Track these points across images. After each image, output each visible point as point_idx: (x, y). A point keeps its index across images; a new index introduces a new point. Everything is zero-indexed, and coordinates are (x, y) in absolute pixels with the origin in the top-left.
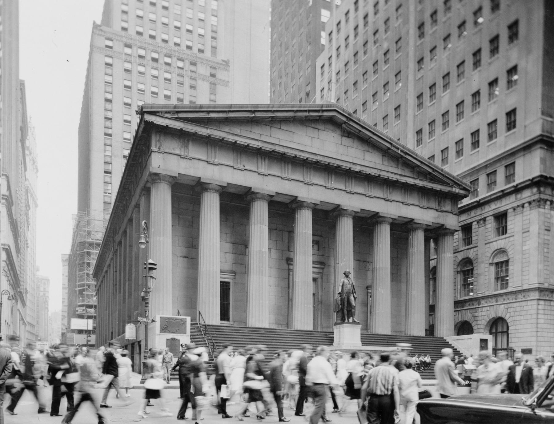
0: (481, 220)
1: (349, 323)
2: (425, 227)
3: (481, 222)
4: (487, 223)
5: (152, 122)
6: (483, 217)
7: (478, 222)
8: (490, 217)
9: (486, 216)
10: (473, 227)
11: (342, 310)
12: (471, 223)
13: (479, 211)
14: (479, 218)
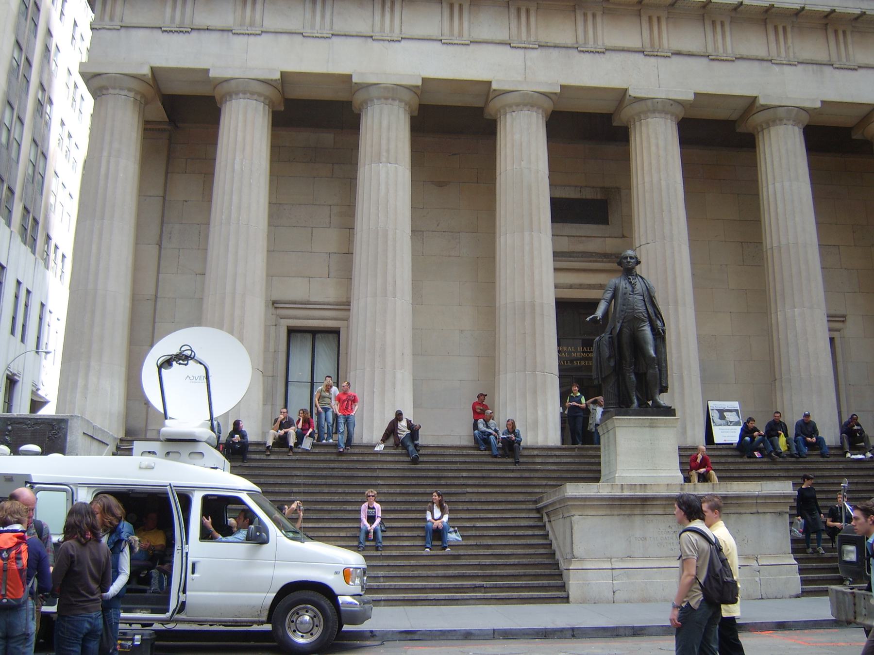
11: (619, 371)
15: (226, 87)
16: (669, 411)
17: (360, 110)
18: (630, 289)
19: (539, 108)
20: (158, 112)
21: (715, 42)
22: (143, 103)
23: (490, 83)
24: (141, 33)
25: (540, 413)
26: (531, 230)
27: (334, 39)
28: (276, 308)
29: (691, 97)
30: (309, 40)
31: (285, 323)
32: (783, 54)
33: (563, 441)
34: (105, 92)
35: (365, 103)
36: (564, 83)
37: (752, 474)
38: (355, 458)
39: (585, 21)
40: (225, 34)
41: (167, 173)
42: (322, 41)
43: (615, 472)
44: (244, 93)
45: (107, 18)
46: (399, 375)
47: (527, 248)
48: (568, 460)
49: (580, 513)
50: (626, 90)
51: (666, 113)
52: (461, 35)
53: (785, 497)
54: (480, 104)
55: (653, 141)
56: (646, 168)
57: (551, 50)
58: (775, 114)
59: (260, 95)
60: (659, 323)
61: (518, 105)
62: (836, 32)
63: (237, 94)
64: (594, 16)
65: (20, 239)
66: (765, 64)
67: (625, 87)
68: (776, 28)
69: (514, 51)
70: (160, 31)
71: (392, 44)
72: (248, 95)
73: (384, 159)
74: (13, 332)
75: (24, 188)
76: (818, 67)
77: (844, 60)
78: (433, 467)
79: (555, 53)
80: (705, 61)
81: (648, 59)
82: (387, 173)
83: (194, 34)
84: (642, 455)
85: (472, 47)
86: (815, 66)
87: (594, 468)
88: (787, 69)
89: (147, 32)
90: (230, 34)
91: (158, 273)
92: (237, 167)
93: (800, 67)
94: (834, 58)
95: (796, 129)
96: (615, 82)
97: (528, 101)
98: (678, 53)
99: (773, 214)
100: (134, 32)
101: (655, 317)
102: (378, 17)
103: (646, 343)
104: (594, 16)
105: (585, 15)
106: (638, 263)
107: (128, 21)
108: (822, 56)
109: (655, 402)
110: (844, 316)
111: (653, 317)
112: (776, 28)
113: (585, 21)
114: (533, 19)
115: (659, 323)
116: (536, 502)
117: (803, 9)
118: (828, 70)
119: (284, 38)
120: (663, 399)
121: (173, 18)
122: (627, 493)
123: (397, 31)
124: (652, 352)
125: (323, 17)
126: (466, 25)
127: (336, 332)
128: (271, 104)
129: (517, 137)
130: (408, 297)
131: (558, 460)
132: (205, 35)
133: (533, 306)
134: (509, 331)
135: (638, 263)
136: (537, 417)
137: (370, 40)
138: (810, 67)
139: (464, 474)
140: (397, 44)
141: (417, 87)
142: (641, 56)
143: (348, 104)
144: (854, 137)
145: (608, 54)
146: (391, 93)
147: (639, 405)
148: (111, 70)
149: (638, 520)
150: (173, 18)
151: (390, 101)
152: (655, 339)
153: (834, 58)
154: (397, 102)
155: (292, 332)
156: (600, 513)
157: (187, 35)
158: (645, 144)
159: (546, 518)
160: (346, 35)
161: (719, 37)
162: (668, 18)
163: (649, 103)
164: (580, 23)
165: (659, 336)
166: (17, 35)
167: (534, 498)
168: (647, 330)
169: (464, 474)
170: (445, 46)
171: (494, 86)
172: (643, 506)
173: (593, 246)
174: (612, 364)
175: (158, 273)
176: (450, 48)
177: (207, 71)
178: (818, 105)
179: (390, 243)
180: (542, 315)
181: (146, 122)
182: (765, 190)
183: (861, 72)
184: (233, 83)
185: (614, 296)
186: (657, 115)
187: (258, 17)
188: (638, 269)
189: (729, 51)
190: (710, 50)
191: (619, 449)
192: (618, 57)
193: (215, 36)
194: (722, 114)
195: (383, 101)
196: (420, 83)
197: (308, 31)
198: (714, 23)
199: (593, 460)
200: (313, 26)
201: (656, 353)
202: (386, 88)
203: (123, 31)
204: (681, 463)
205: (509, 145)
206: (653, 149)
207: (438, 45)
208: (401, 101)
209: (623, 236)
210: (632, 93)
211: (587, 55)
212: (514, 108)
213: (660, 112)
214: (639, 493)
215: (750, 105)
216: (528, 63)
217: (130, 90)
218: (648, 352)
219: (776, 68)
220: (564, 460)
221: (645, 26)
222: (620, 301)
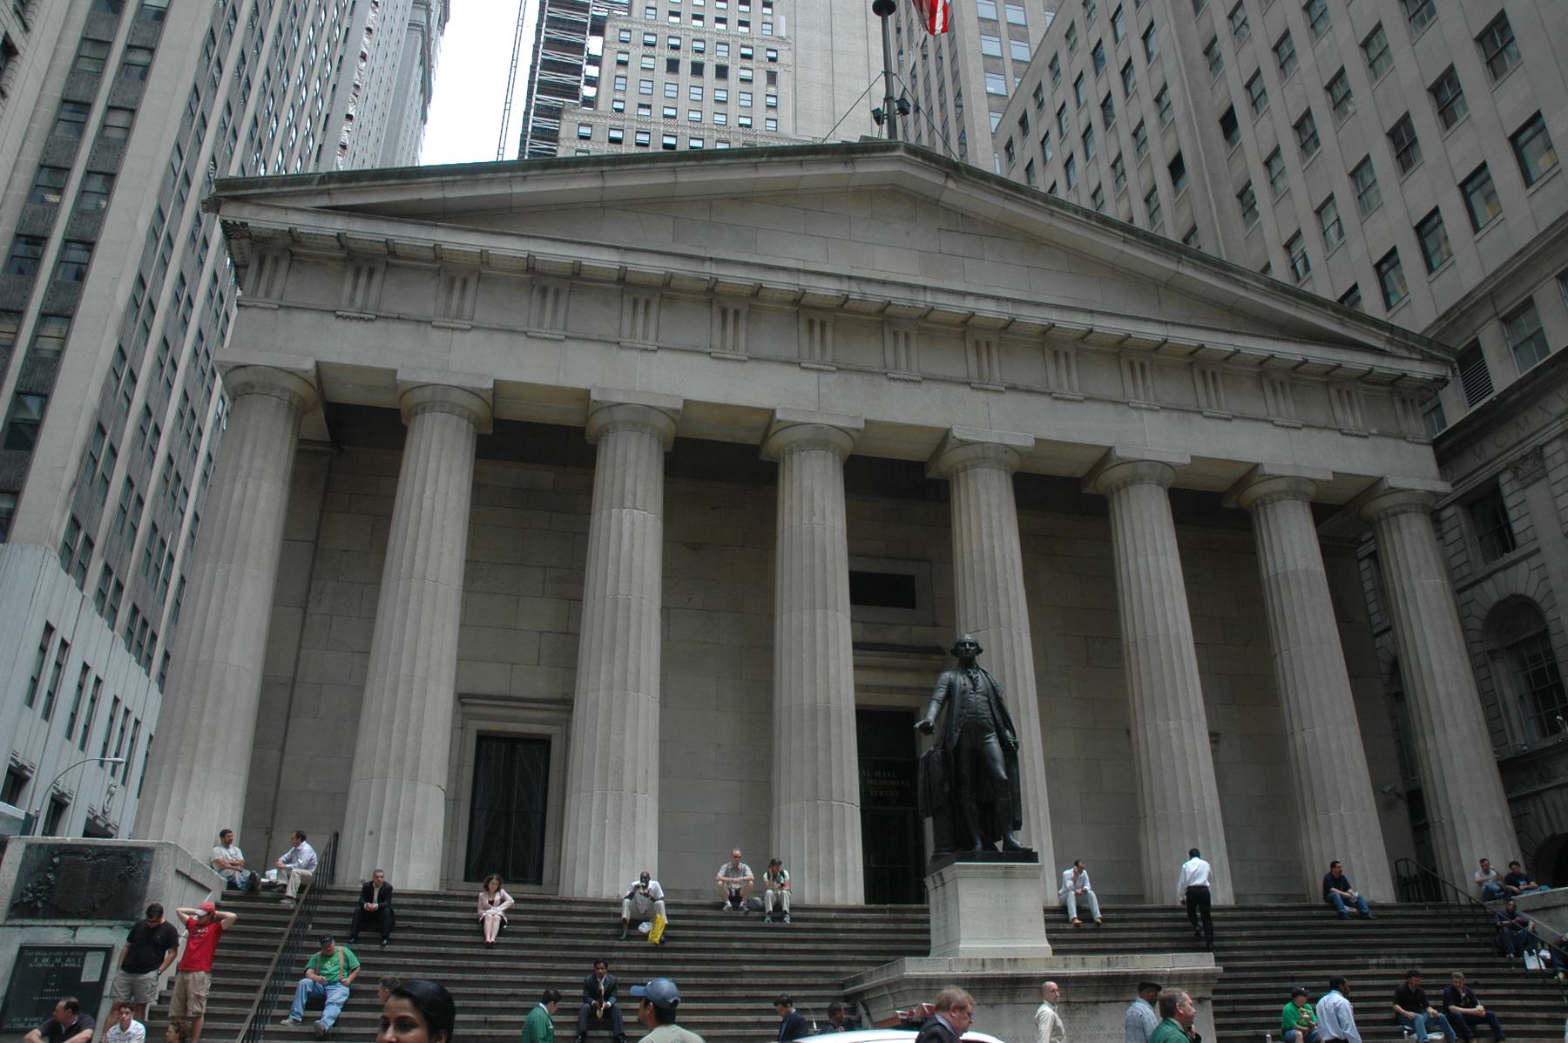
0: (1524, 458)
1: (990, 855)
2: (1311, 489)
3: (1529, 466)
4: (1549, 464)
5: (244, 225)
6: (1528, 449)
7: (1514, 467)
8: (1557, 445)
9: (1540, 442)
10: (1506, 490)
12: (1495, 478)
13: (1508, 436)
14: (1518, 456)
15: (418, 396)
16: (1029, 856)
17: (598, 438)
18: (969, 685)
20: (316, 427)
22: (298, 411)
23: (773, 411)
25: (837, 859)
26: (826, 607)
27: (568, 343)
28: (463, 704)
29: (1030, 443)
31: (475, 726)
32: (1142, 396)
33: (867, 901)
35: (604, 431)
36: (870, 417)
37: (1130, 945)
38: (578, 919)
39: (896, 341)
40: (422, 327)
41: (322, 511)
42: (551, 344)
43: (958, 941)
45: (261, 292)
46: (640, 803)
47: (819, 632)
48: (881, 926)
50: (947, 432)
52: (735, 348)
53: (1206, 976)
54: (753, 440)
56: (974, 532)
60: (1008, 733)
62: (1203, 373)
65: (94, 607)
66: (1120, 408)
67: (947, 426)
68: (1132, 365)
69: (805, 373)
71: (645, 354)
73: (628, 504)
74: (69, 735)
75: (108, 539)
78: (691, 933)
79: (856, 379)
80: (1047, 400)
81: (975, 393)
82: (633, 523)
83: (379, 324)
84: (991, 920)
88: (1146, 415)
91: (300, 648)
92: (427, 503)
93: (1163, 414)
94: (1203, 402)
96: (937, 420)
97: (820, 439)
98: (1013, 388)
99: (1135, 597)
100: (296, 315)
101: (1003, 723)
102: (627, 320)
103: (993, 759)
104: (907, 335)
105: (895, 334)
106: (979, 651)
107: (290, 299)
109: (1009, 845)
111: (1001, 723)
113: (896, 341)
115: (1008, 733)
116: (842, 986)
118: (1197, 419)
119: (501, 338)
120: (1019, 839)
121: (352, 300)
122: (990, 971)
124: (1003, 773)
125: (555, 313)
126: (742, 336)
127: (544, 743)
128: (476, 422)
129: (807, 483)
130: (655, 692)
131: (865, 926)
132: (398, 326)
133: (827, 710)
134: (791, 746)
135: (979, 651)
136: (827, 865)
137: (615, 348)
138: (1175, 415)
139: (737, 945)
140: (651, 355)
141: (677, 411)
142: (967, 389)
143: (580, 431)
144: (1230, 504)
145: (925, 385)
146: (640, 418)
147: (985, 847)
149: (1006, 1010)
150: (352, 300)
152: (1005, 756)
155: (483, 738)
157: (369, 325)
158: (972, 501)
159: (862, 1010)
160: (584, 339)
161: (1063, 371)
166: (121, 339)
167: (841, 980)
168: (994, 742)
169: (737, 945)
173: (895, 636)
174: (947, 789)
175: (300, 648)
176: (722, 364)
177: (395, 372)
178: (1188, 460)
179: (633, 617)
180: (840, 722)
181: (301, 441)
182: (1123, 566)
183: (1235, 423)
184: (428, 391)
185: (949, 696)
187: (468, 307)
188: (980, 660)
189: (1076, 388)
191: (962, 909)
192: (937, 390)
194: (1063, 469)
196: (680, 405)
197: (533, 330)
198: (1056, 354)
199: (919, 926)
200: (540, 325)
201: (1007, 773)
203: (281, 313)
204: (1048, 931)
205: (796, 494)
206: (984, 507)
207: (706, 359)
209: (935, 625)
210: (959, 433)
211: (898, 385)
214: (1008, 971)
215: (1105, 457)
218: (998, 773)
219: (1135, 414)
220: (874, 926)
222: (957, 702)
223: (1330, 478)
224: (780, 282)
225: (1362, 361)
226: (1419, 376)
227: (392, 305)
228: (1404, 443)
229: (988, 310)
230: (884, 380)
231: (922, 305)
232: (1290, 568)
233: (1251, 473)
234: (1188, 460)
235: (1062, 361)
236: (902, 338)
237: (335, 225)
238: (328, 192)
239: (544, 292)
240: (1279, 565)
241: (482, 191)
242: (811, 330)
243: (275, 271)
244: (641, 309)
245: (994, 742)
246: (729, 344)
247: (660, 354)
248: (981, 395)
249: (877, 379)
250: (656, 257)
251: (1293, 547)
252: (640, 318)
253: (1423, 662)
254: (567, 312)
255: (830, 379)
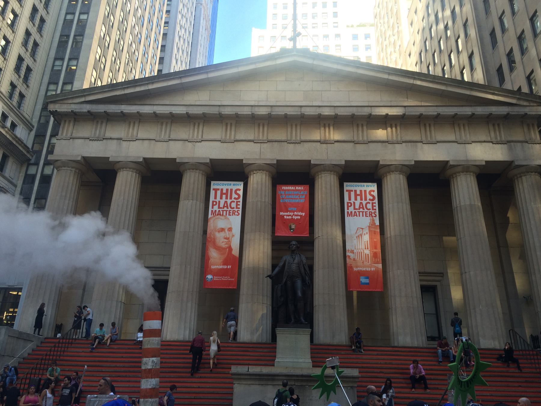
5: (56, 111)
19: (267, 171)
21: (358, 135)
24: (80, 141)
30: (159, 143)
34: (60, 169)
39: (292, 128)
40: (119, 141)
44: (126, 168)
49: (237, 382)
51: (331, 171)
53: (353, 377)
55: (324, 185)
56: (320, 200)
57: (274, 143)
58: (389, 168)
59: (134, 169)
61: (256, 170)
63: (123, 168)
64: (296, 126)
66: (384, 144)
67: (310, 159)
70: (88, 140)
72: (128, 169)
76: (414, 143)
77: (429, 139)
79: (276, 144)
80: (352, 144)
83: (105, 141)
85: (236, 143)
86: (412, 143)
87: (137, 365)
88: (397, 145)
89: (82, 140)
90: (122, 141)
93: (404, 144)
94: (424, 139)
95: (401, 176)
96: (305, 157)
97: (260, 168)
100: (77, 141)
102: (191, 131)
104: (296, 126)
105: (292, 125)
108: (417, 138)
110: (443, 273)
112: (425, 125)
113: (292, 128)
114: (266, 129)
117: (404, 115)
118: (419, 145)
119: (147, 142)
121: (95, 134)
123: (200, 137)
124: (300, 294)
125: (165, 132)
126: (233, 133)
137: (187, 142)
138: (410, 143)
140: (199, 143)
141: (208, 163)
142: (319, 143)
146: (196, 166)
148: (63, 158)
150: (95, 134)
151: (195, 170)
153: (424, 139)
154: (198, 171)
156: (257, 383)
158: (320, 187)
161: (360, 132)
162: (334, 124)
163: (322, 166)
164: (289, 129)
165: (308, 285)
170: (222, 144)
171: (244, 162)
172: (273, 380)
174: (282, 299)
178: (413, 163)
183: (438, 144)
186: (326, 172)
190: (355, 139)
193: (115, 141)
195: (191, 170)
197: (158, 138)
202: (192, 164)
203: (71, 140)
206: (324, 189)
207: (219, 143)
208: (200, 170)
211: (292, 145)
212: (255, 172)
213: (328, 171)
216: (262, 150)
217: (72, 168)
219: (390, 146)
221: (322, 129)
223: (484, 163)
224: (246, 111)
225: (503, 110)
226: (534, 113)
227: (108, 134)
228: (527, 144)
229: (326, 112)
230: (286, 143)
231: (299, 113)
232: (462, 204)
233: (445, 164)
234: (413, 163)
235: (360, 128)
236: (294, 126)
237: (86, 108)
238: (85, 96)
239: (162, 124)
240: (458, 203)
241: (138, 89)
242: (259, 128)
243: (69, 126)
244: (196, 127)
245: (299, 283)
246: (228, 136)
247: (203, 142)
248: (324, 145)
249: (283, 143)
250: (200, 107)
251: (466, 193)
252: (196, 130)
253: (531, 242)
254: (170, 131)
255: (265, 145)
